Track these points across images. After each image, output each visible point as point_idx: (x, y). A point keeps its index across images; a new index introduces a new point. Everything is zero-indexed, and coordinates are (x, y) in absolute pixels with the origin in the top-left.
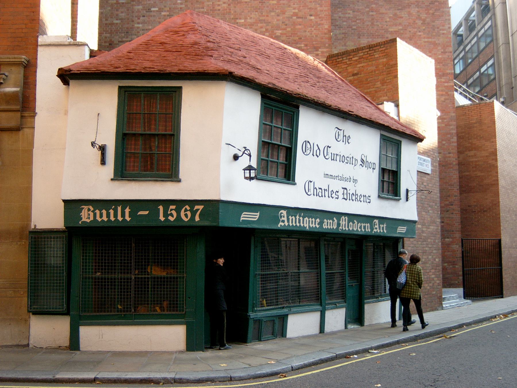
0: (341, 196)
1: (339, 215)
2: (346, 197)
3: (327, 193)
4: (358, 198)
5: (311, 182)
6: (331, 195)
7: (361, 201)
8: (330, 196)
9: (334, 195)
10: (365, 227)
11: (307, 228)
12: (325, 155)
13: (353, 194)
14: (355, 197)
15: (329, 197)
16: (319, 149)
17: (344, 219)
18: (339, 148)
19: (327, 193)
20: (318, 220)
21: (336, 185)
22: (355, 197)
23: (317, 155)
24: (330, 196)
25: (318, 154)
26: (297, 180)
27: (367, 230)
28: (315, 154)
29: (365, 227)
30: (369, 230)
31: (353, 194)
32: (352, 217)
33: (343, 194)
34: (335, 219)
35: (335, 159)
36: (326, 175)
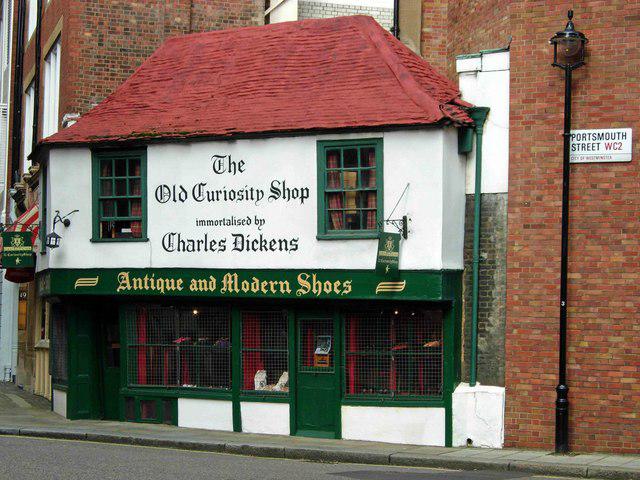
0: (230, 245)
1: (220, 273)
2: (239, 246)
3: (202, 246)
4: (268, 246)
5: (173, 234)
6: (211, 246)
7: (273, 250)
8: (208, 247)
9: (216, 247)
10: (277, 287)
11: (162, 291)
12: (197, 195)
13: (256, 241)
14: (263, 244)
15: (206, 250)
16: (183, 190)
17: (230, 277)
18: (228, 181)
19: (202, 246)
20: (180, 281)
21: (225, 233)
22: (263, 244)
23: (180, 199)
24: (208, 247)
25: (183, 197)
26: (149, 235)
27: (282, 291)
28: (177, 198)
29: (277, 287)
30: (289, 291)
31: (256, 241)
32: (245, 274)
33: (235, 243)
34: (254, 278)
35: (215, 198)
36: (201, 223)
